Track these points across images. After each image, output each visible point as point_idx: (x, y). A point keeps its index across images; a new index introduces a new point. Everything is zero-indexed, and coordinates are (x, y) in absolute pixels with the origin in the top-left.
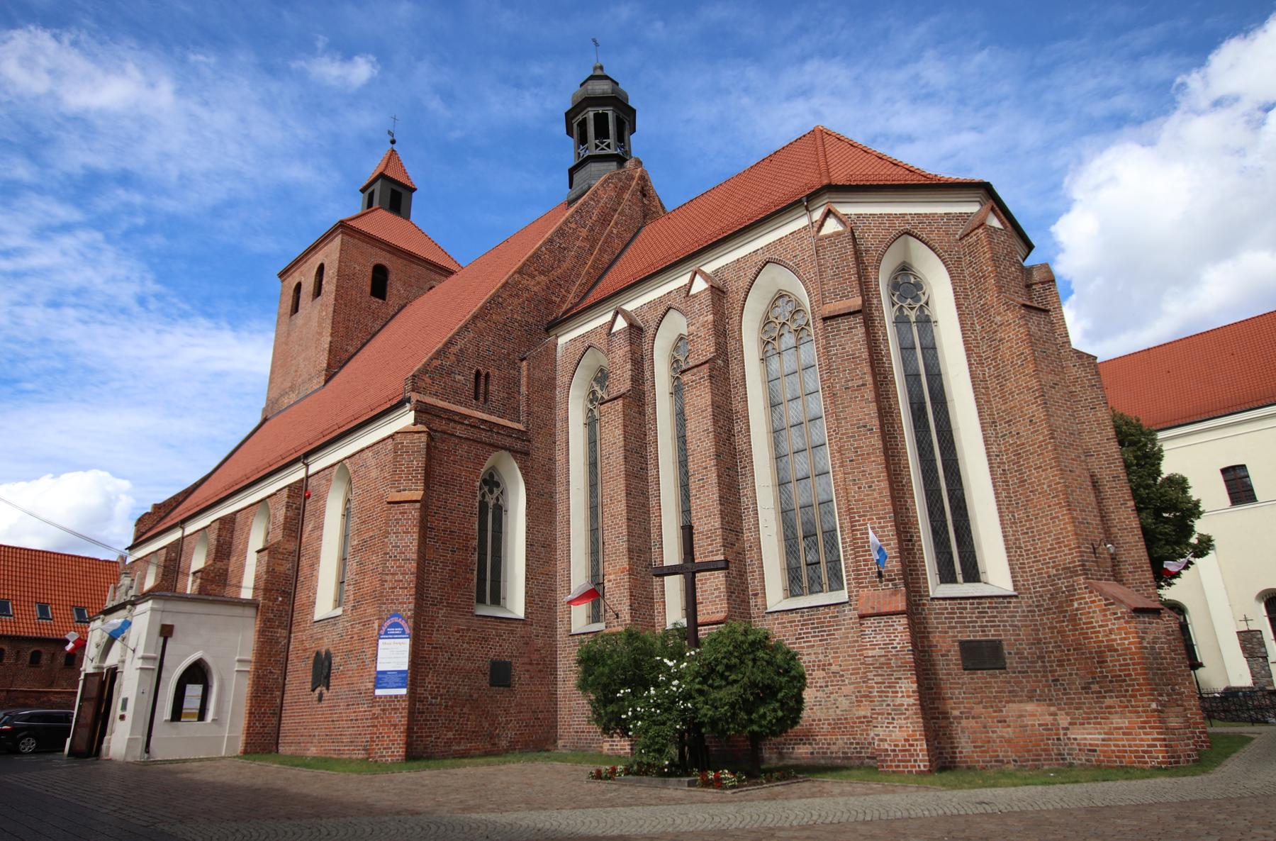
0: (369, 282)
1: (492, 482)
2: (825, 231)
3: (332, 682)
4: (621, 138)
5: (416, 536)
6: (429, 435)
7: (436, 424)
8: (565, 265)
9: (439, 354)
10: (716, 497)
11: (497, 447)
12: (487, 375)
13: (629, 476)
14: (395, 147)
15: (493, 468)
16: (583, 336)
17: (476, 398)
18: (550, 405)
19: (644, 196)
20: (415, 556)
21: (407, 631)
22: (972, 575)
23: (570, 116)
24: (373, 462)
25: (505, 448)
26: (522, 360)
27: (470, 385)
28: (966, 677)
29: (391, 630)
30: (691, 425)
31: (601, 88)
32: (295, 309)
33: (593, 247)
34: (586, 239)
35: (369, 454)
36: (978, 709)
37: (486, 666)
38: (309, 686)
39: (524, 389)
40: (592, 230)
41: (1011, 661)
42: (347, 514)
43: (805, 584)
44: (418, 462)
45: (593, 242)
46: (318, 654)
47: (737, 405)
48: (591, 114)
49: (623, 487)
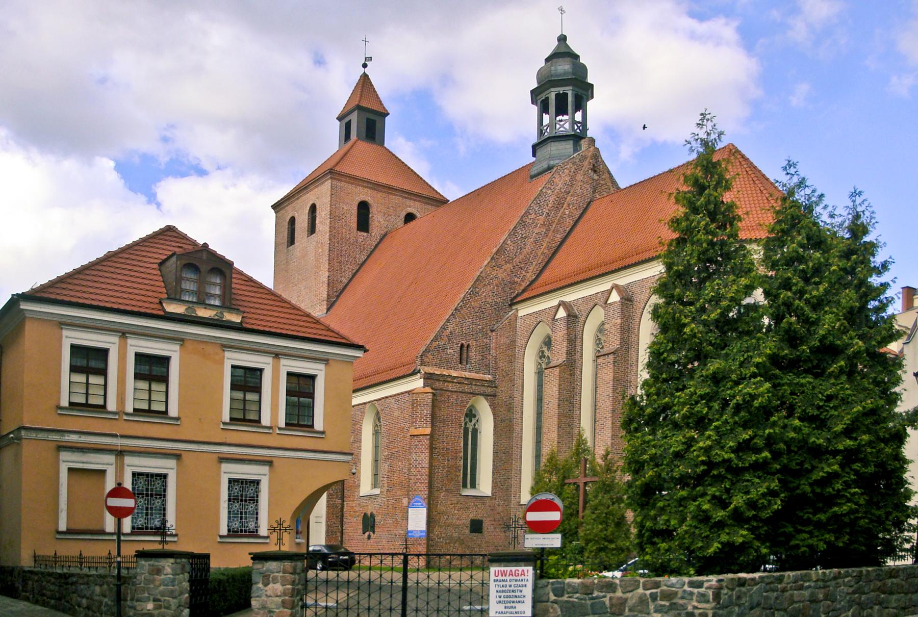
3: (376, 530)
6: (434, 395)
7: (438, 385)
10: (610, 435)
13: (560, 416)
15: (472, 406)
16: (536, 313)
25: (481, 394)
26: (492, 331)
38: (361, 531)
42: (376, 433)
49: (556, 423)
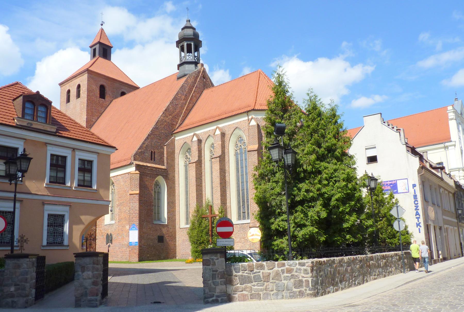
0: (99, 93)
1: (157, 185)
2: (251, 124)
5: (138, 203)
8: (177, 111)
11: (158, 175)
14: (103, 27)
15: (157, 180)
17: (152, 160)
18: (173, 160)
19: (204, 78)
20: (138, 209)
23: (178, 43)
24: (122, 180)
27: (150, 156)
30: (214, 174)
31: (189, 32)
32: (68, 100)
33: (186, 102)
34: (184, 99)
35: (120, 177)
38: (105, 243)
39: (165, 155)
40: (186, 96)
43: (242, 217)
44: (137, 182)
46: (107, 234)
47: (227, 168)
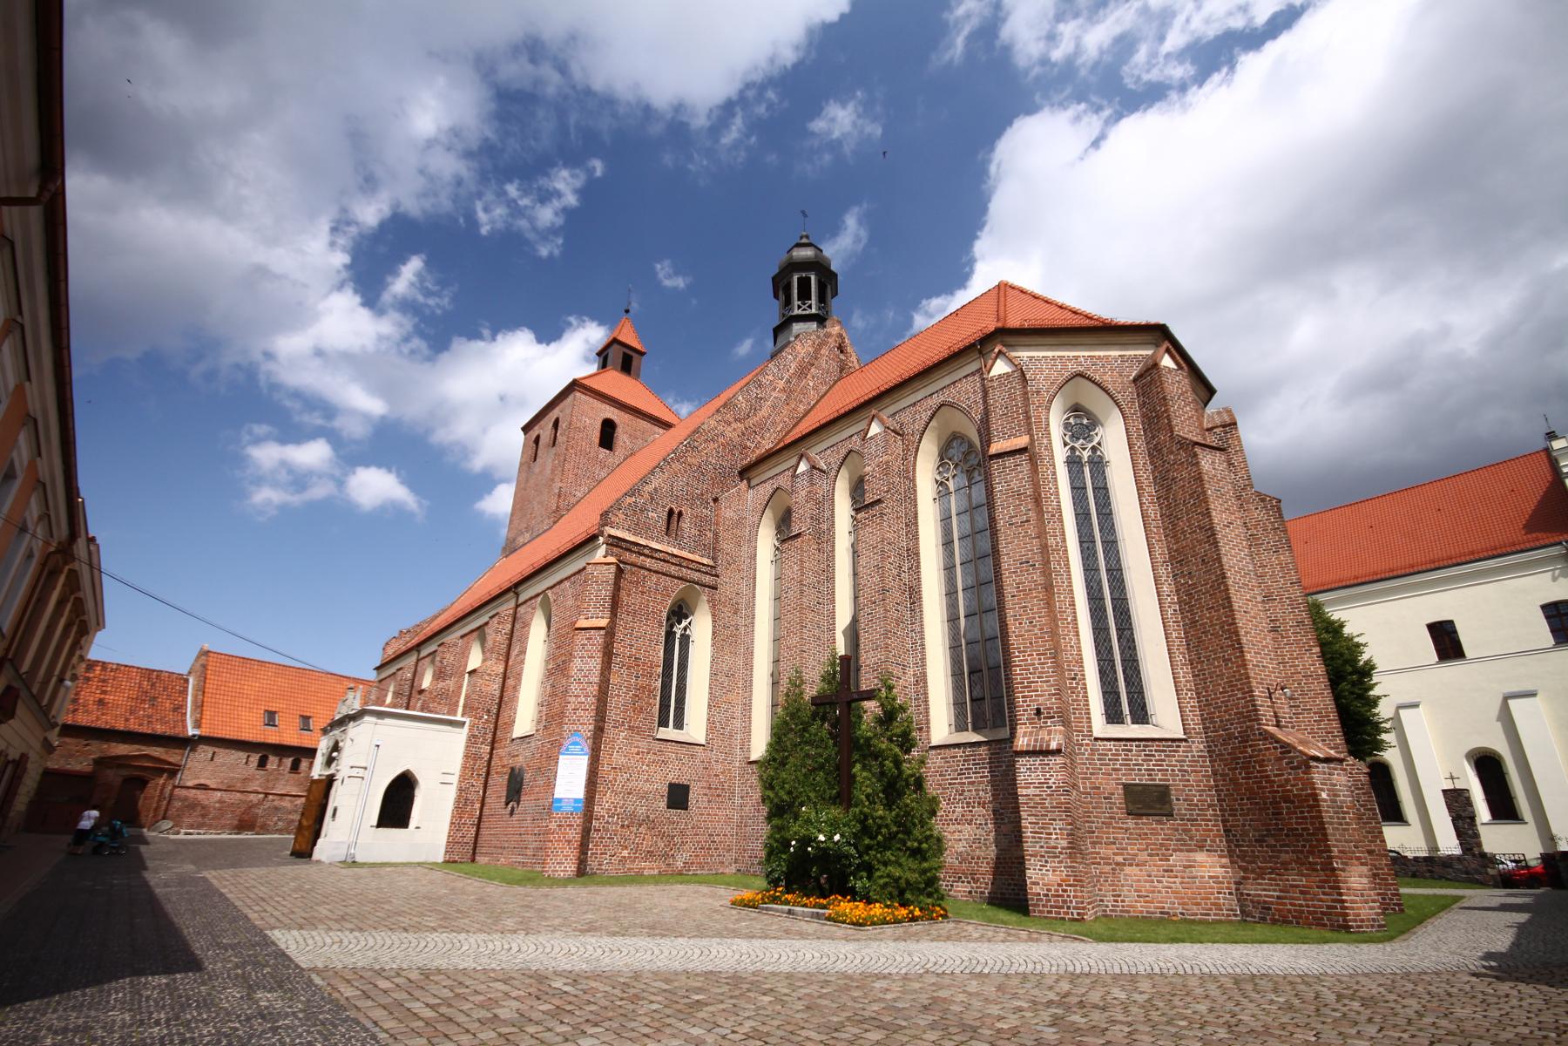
4: (822, 299)
7: (628, 556)
8: (761, 413)
9: (632, 492)
12: (680, 514)
20: (597, 680)
21: (586, 749)
22: (1141, 714)
23: (776, 280)
24: (570, 592)
27: (662, 523)
28: (1130, 823)
29: (572, 748)
34: (783, 390)
35: (567, 584)
36: (1143, 856)
37: (665, 790)
40: (789, 381)
41: (1179, 806)
45: (788, 391)
48: (795, 278)
